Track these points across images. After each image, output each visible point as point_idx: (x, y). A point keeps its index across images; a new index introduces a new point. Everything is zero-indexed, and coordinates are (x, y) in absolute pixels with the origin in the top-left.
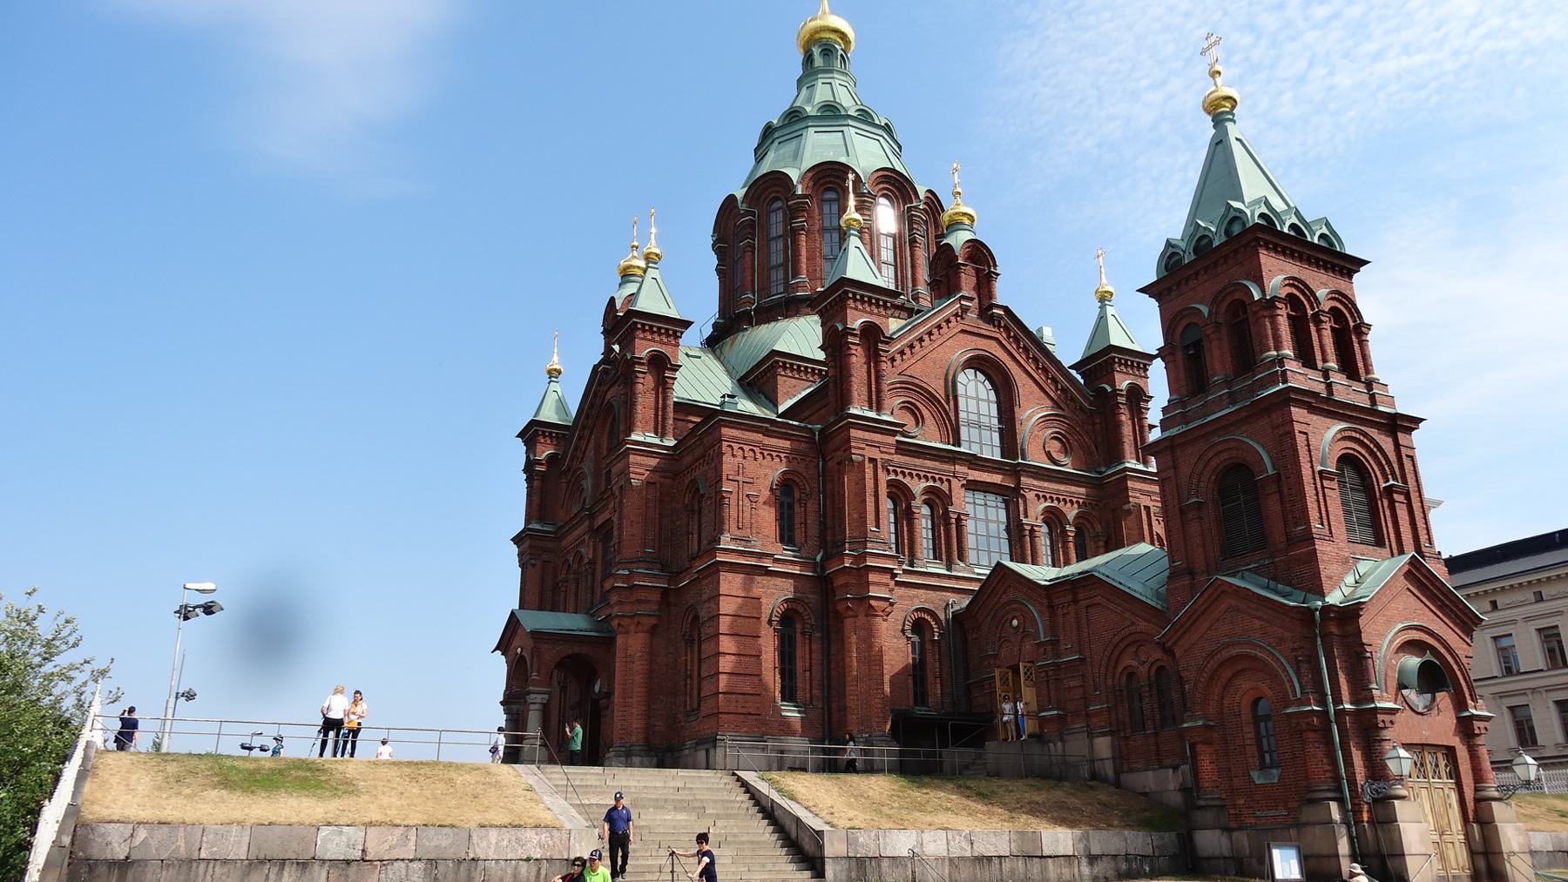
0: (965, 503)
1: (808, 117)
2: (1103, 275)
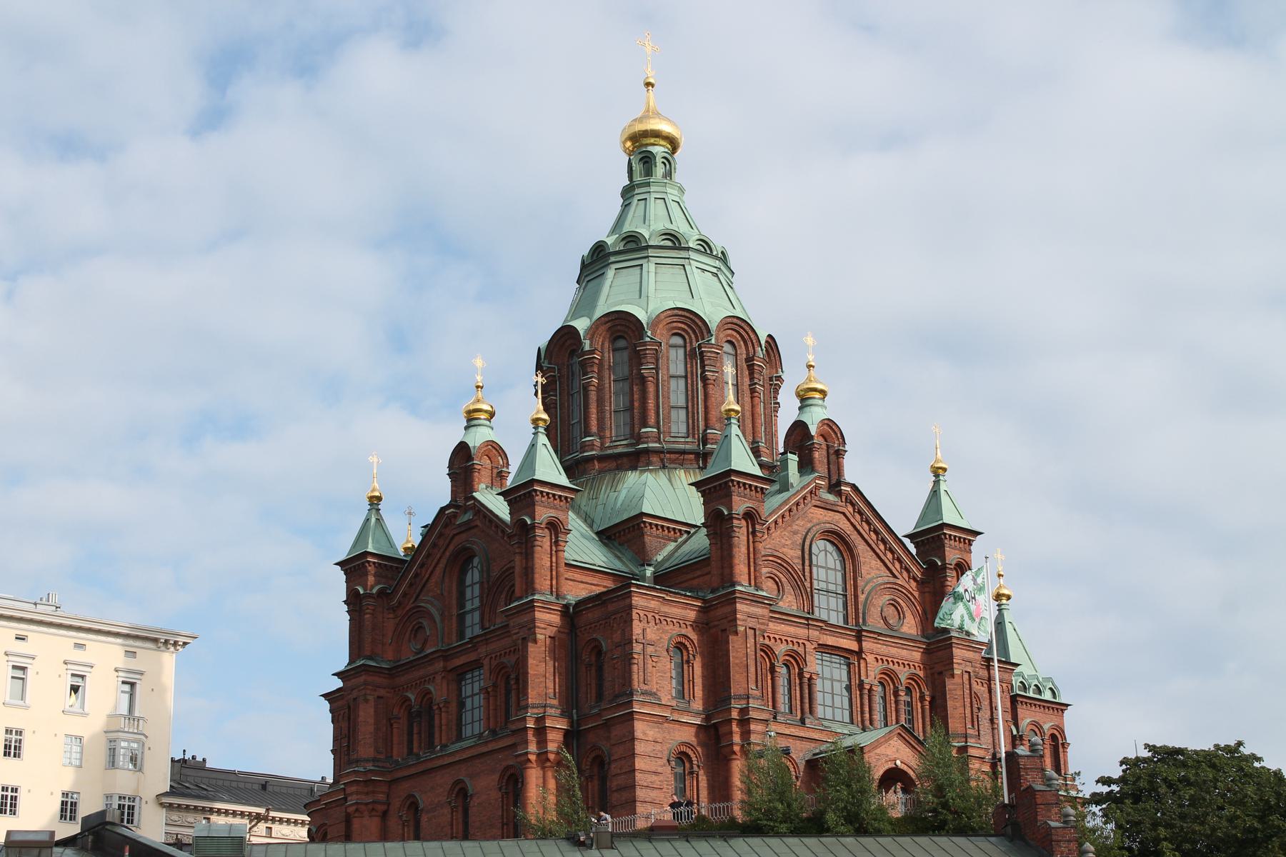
0: (815, 664)
1: (648, 247)
2: (938, 450)
